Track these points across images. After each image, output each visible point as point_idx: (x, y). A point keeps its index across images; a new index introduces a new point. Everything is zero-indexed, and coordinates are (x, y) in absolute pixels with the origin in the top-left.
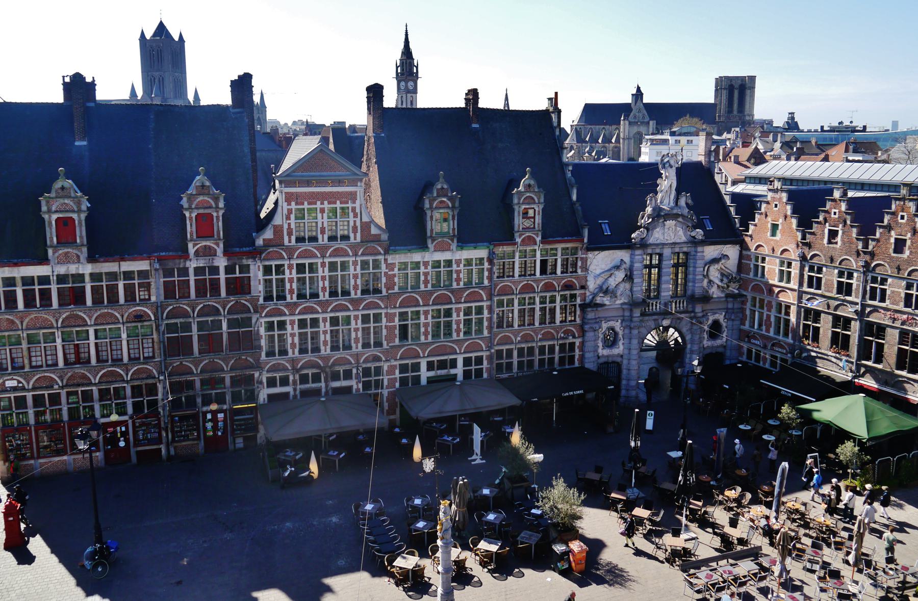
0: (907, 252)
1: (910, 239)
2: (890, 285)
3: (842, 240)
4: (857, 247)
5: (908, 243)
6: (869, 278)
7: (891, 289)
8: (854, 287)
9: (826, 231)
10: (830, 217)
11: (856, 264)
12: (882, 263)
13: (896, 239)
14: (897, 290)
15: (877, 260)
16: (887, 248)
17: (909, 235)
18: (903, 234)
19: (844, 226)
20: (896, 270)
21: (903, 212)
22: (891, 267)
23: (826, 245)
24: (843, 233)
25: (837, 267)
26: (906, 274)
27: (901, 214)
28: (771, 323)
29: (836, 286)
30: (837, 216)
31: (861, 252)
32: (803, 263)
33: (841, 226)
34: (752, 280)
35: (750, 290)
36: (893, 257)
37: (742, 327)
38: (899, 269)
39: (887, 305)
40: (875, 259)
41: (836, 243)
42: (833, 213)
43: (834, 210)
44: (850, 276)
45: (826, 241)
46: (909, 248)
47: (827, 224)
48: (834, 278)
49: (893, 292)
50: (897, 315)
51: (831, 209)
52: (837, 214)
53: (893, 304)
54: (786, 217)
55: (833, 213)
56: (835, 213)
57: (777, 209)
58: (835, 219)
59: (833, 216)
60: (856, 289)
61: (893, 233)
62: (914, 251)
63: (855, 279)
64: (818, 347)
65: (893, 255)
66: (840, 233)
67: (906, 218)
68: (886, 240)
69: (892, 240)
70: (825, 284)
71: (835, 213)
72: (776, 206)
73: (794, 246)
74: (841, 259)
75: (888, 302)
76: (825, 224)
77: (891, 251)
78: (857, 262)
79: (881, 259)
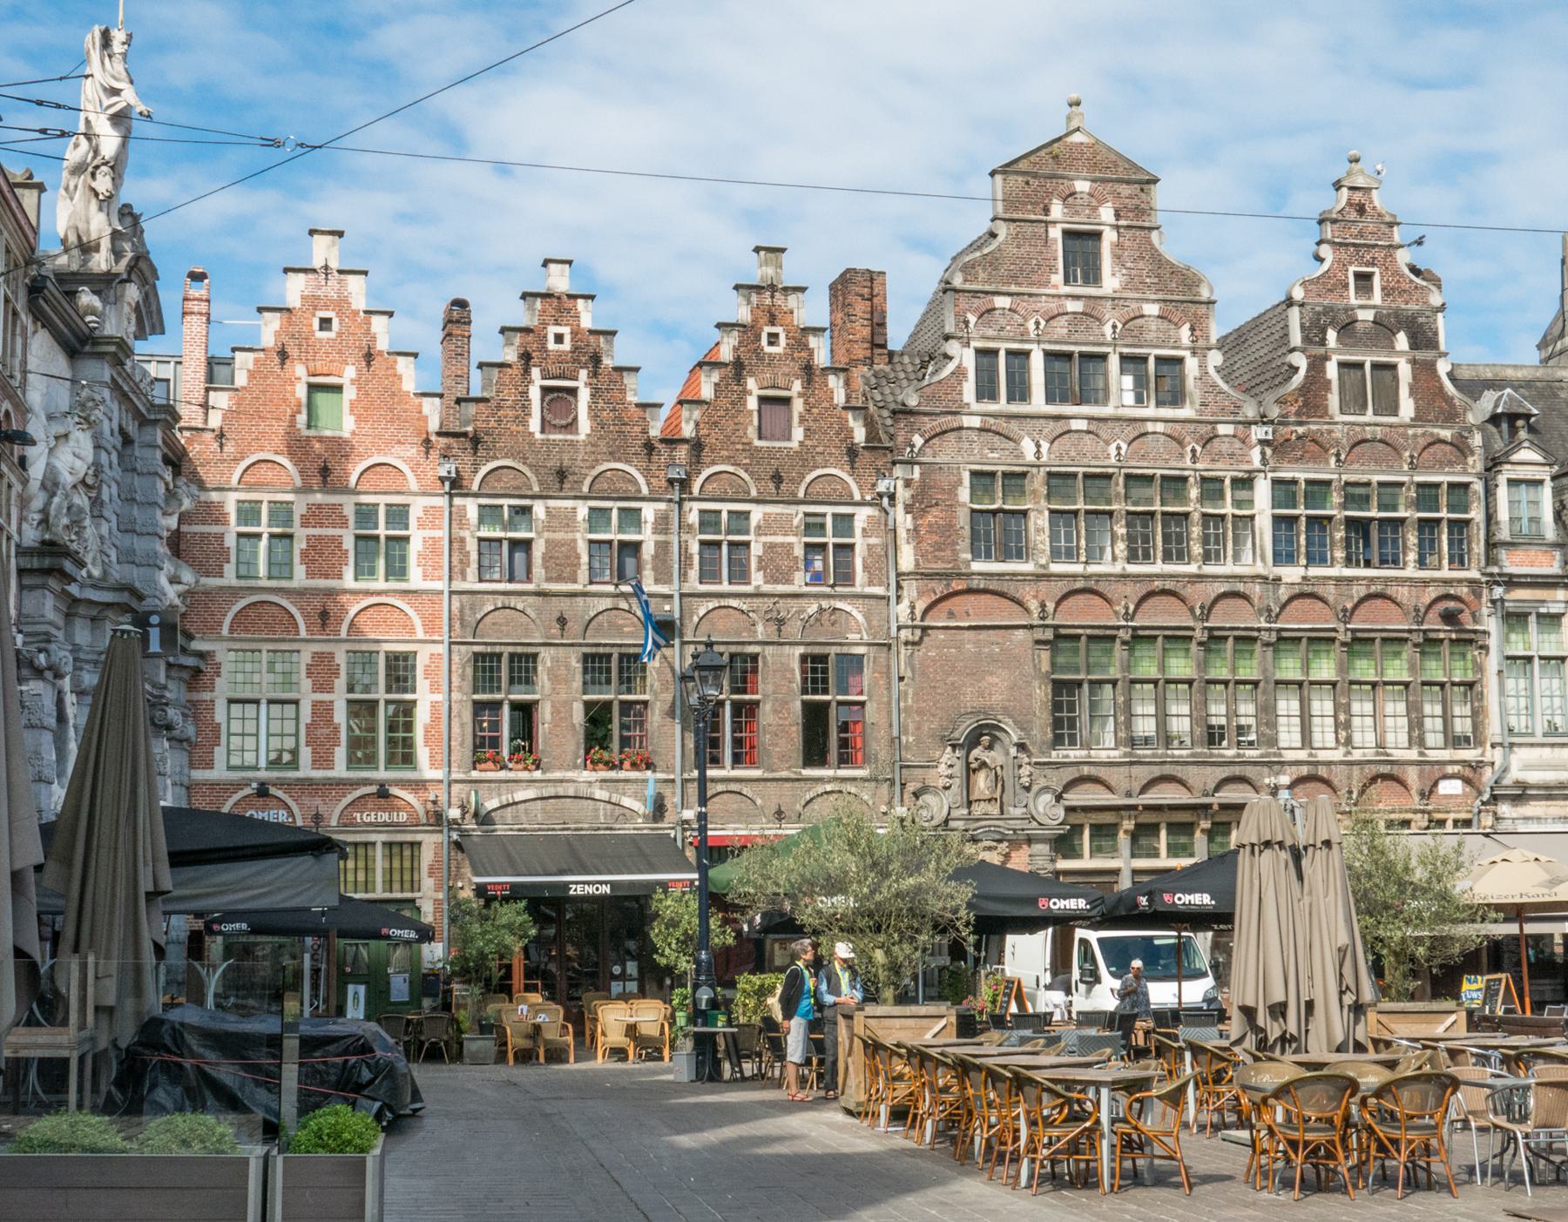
0: (798, 433)
1: (800, 395)
2: (759, 527)
3: (594, 414)
4: (645, 431)
5: (798, 406)
6: (693, 518)
7: (764, 539)
8: (648, 551)
9: (535, 393)
10: (543, 348)
11: (649, 484)
12: (731, 469)
13: (763, 400)
14: (779, 539)
15: (713, 463)
16: (739, 427)
17: (797, 386)
18: (781, 381)
19: (594, 374)
20: (771, 485)
21: (773, 324)
22: (758, 480)
23: (538, 436)
24: (593, 395)
25: (585, 498)
26: (801, 494)
27: (768, 329)
28: (336, 729)
29: (585, 559)
30: (567, 346)
31: (657, 445)
32: (457, 501)
33: (583, 374)
34: (235, 592)
35: (225, 632)
36: (758, 449)
37: (199, 775)
38: (777, 478)
39: (758, 587)
40: (707, 460)
41: (571, 426)
42: (551, 338)
43: (552, 330)
44: (631, 518)
45: (534, 424)
46: (802, 420)
47: (535, 373)
48: (578, 536)
49: (770, 547)
50: (794, 605)
51: (545, 325)
52: (567, 339)
53: (776, 581)
54: (369, 357)
55: (551, 338)
56: (559, 338)
57: (332, 335)
58: (560, 354)
59: (551, 345)
60: (655, 557)
61: (751, 383)
62: (814, 426)
63: (648, 529)
64: (538, 765)
65: (757, 443)
66: (584, 395)
67: (782, 340)
68: (733, 403)
69: (752, 403)
70: (546, 558)
71: (559, 338)
72: (325, 323)
73: (413, 451)
74: (595, 472)
75: (757, 579)
76: (527, 371)
77: (752, 432)
78: (647, 473)
79: (728, 460)
